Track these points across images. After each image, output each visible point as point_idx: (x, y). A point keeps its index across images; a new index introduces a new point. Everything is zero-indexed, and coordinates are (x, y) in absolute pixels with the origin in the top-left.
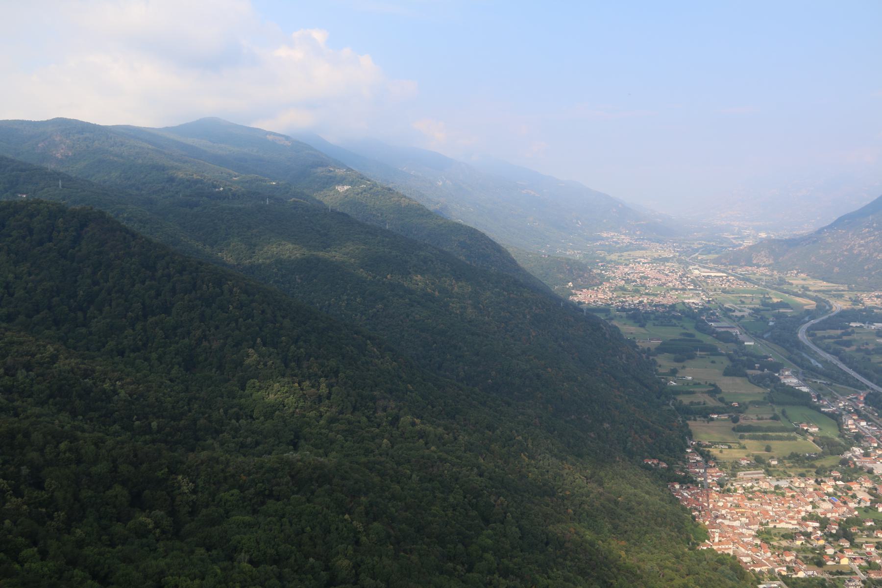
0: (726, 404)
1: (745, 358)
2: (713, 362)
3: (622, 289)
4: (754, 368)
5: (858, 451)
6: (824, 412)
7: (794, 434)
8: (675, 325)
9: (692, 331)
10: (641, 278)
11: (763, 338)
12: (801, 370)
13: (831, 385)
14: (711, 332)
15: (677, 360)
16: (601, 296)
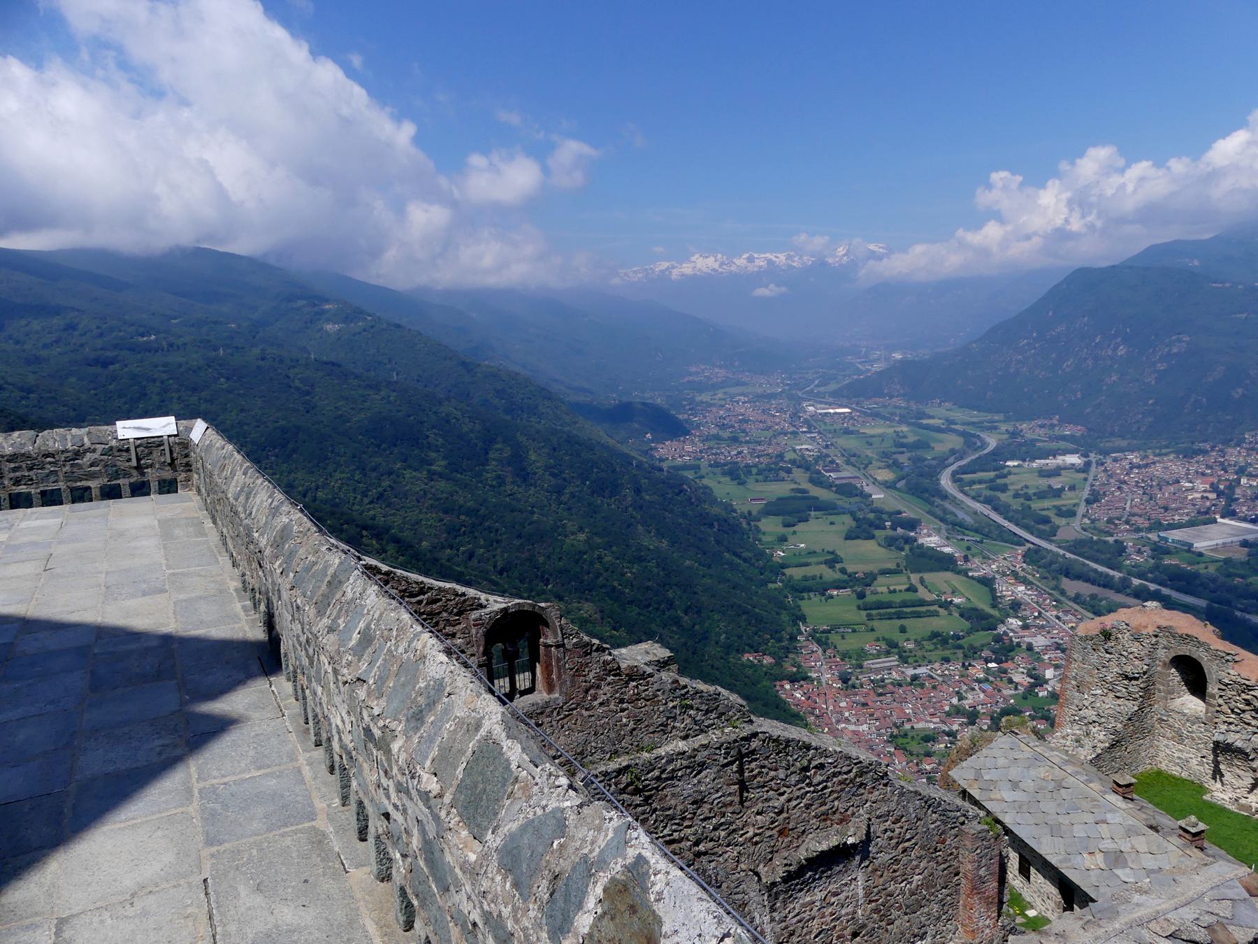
0: (850, 576)
1: (871, 516)
2: (832, 523)
3: (717, 438)
4: (885, 528)
5: (1014, 623)
6: (972, 578)
7: (935, 608)
8: (783, 480)
9: (805, 485)
10: (740, 421)
11: (896, 488)
12: (943, 526)
13: (981, 542)
14: (829, 486)
15: (786, 525)
16: (688, 448)
